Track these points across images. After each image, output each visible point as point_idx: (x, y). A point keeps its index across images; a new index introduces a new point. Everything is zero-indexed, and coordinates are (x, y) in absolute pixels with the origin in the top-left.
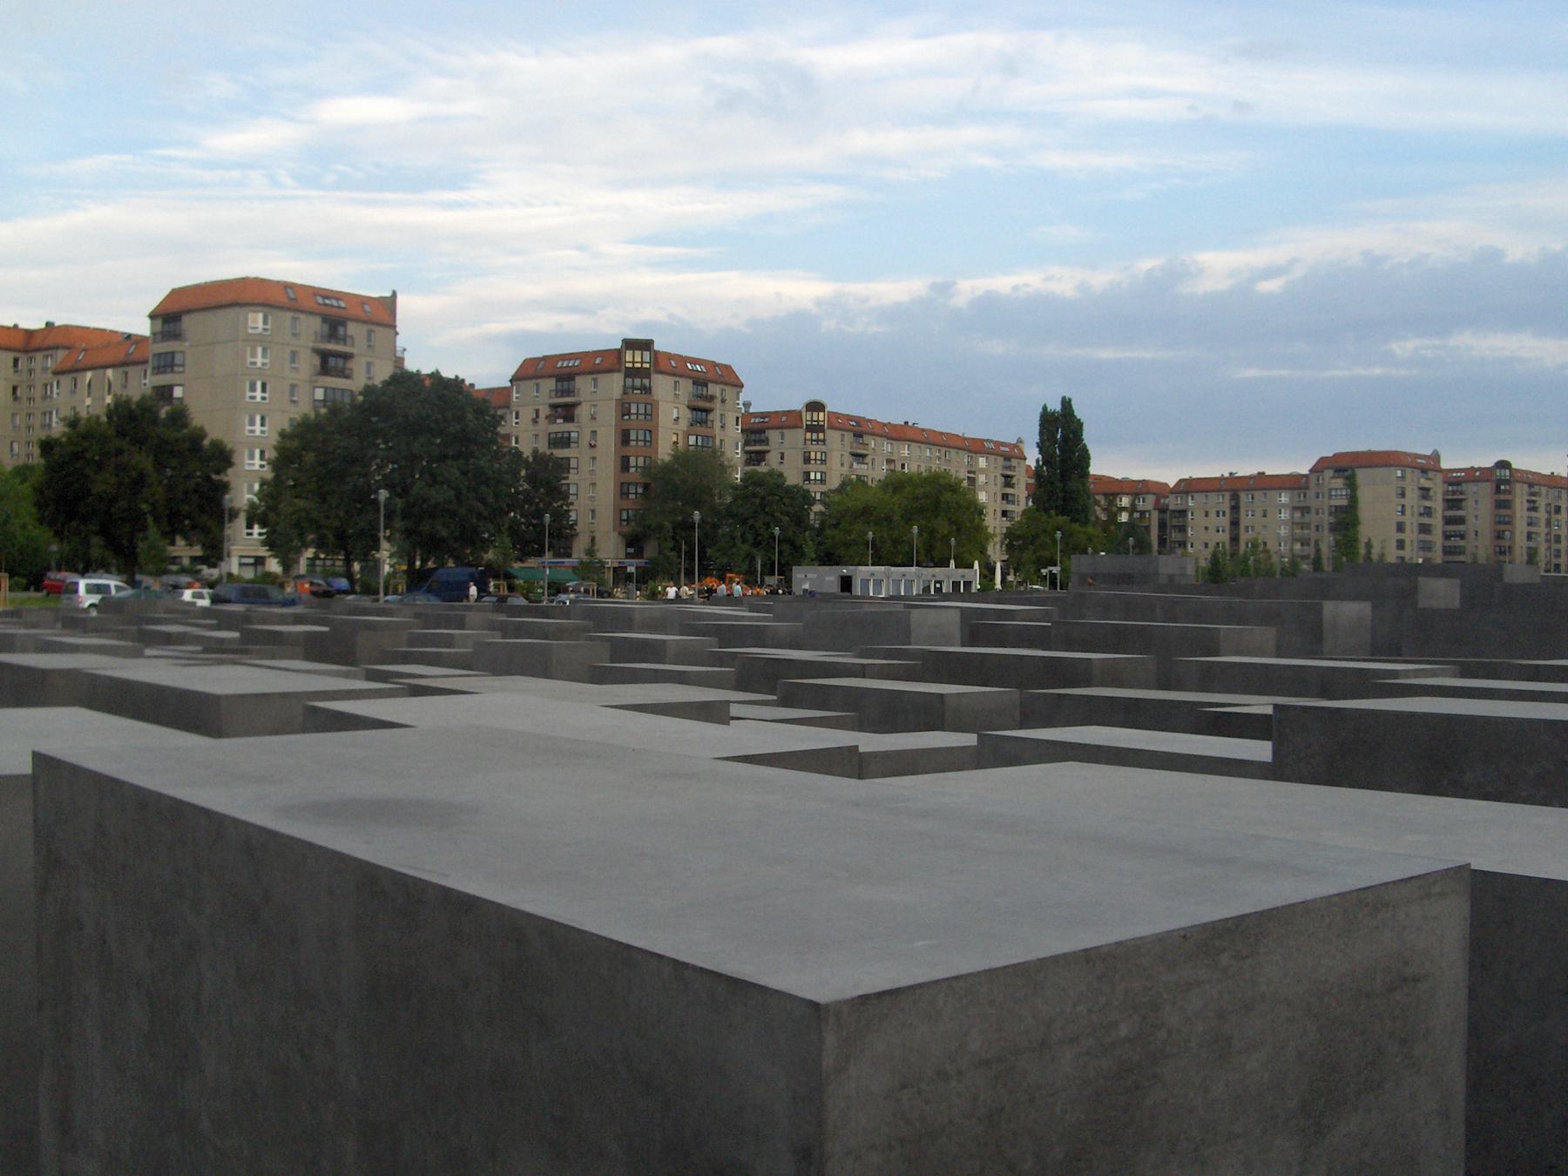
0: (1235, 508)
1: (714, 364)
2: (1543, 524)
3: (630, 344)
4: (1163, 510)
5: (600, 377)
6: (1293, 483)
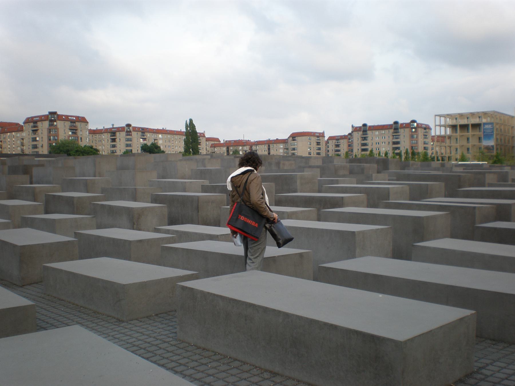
0: (269, 149)
1: (79, 117)
2: (430, 149)
5: (43, 122)
6: (284, 141)
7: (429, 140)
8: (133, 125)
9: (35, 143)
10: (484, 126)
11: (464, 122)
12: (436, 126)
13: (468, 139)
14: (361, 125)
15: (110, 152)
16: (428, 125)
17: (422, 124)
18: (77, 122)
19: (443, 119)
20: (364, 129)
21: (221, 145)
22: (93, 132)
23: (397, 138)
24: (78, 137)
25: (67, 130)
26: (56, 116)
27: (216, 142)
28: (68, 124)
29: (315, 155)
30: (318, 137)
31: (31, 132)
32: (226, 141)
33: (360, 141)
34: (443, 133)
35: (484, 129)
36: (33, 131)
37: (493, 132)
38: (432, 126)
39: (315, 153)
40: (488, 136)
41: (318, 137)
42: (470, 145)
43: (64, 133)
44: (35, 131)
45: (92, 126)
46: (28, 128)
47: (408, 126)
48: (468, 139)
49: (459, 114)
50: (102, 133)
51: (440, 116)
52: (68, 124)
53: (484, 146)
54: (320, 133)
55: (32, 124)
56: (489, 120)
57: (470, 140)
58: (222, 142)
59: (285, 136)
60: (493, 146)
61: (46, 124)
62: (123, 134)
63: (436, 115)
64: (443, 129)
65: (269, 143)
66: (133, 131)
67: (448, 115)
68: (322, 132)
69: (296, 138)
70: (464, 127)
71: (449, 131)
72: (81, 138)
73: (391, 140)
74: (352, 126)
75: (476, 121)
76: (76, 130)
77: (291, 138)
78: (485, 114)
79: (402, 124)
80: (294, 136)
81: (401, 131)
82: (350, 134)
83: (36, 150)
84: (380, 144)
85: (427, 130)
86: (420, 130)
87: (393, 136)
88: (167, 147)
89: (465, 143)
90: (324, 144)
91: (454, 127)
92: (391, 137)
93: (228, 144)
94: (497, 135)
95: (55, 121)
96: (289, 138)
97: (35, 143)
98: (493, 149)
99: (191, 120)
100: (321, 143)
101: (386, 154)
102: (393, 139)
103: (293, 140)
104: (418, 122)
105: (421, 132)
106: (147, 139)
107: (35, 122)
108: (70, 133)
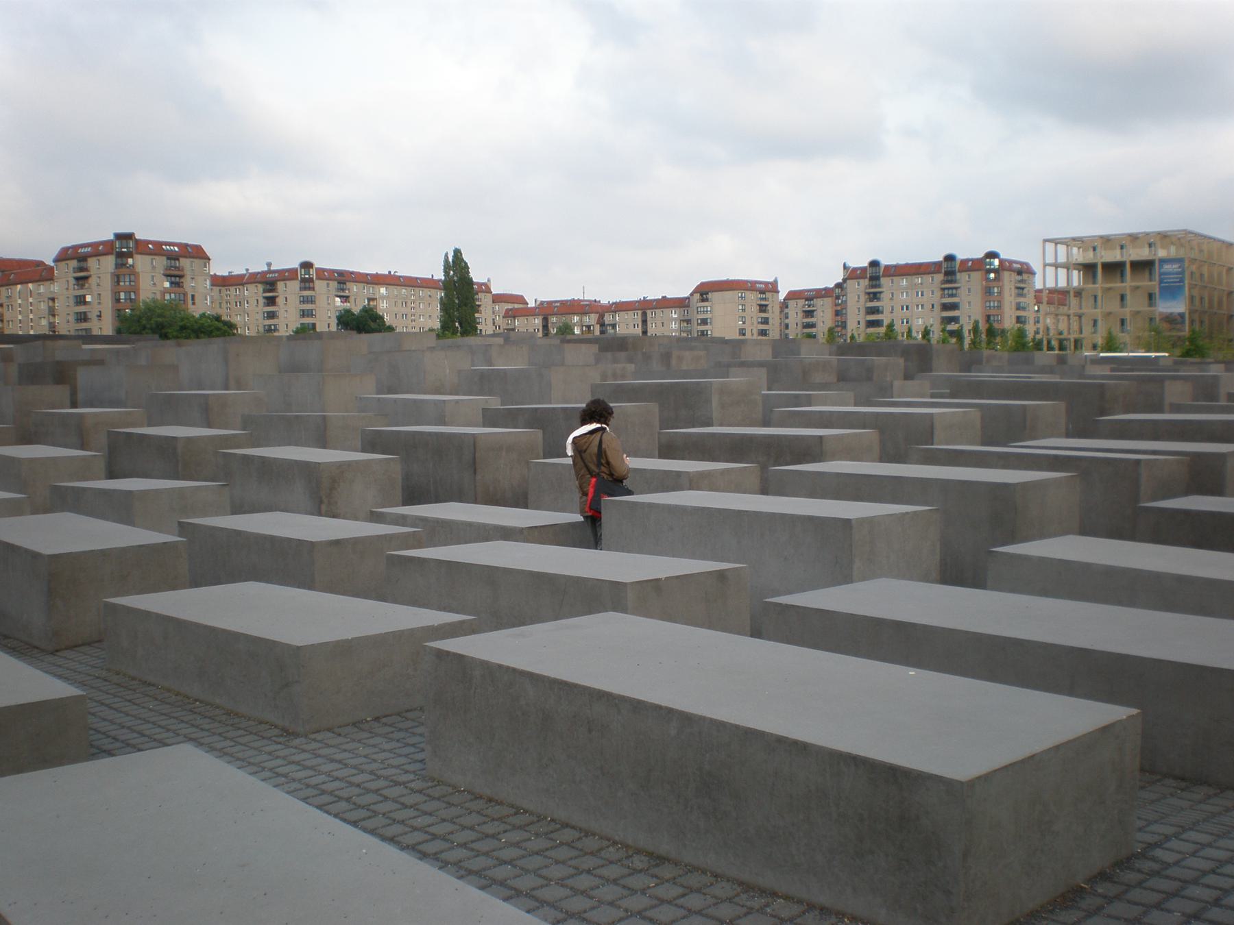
0: (644, 322)
1: (187, 245)
2: (1032, 322)
3: (119, 237)
4: (602, 325)
5: (101, 258)
6: (681, 303)
7: (1029, 299)
8: (317, 265)
9: (82, 309)
10: (1161, 267)
11: (1114, 256)
12: (1045, 265)
13: (1122, 298)
14: (866, 264)
15: (261, 330)
16: (1027, 264)
17: (1011, 262)
18: (181, 258)
19: (1062, 249)
20: (874, 274)
21: (530, 313)
22: (222, 282)
23: (952, 296)
24: (185, 294)
25: (159, 277)
26: (131, 244)
27: (516, 306)
28: (161, 262)
29: (755, 337)
30: (762, 292)
31: (72, 281)
32: (542, 303)
33: (863, 303)
34: (1062, 283)
35: (1160, 274)
36: (77, 279)
37: (1182, 280)
38: (1036, 266)
39: (755, 332)
40: (1171, 291)
41: (762, 292)
42: (1126, 312)
43: (151, 284)
44: (81, 281)
45: (219, 268)
46: (67, 272)
47: (977, 265)
48: (1122, 298)
49: (1101, 237)
50: (243, 285)
51: (1056, 242)
52: (161, 262)
53: (1161, 314)
54: (767, 284)
55: (74, 263)
56: (1173, 252)
57: (1128, 297)
58: (531, 304)
59: (683, 290)
60: (1182, 315)
61: (109, 262)
62: (294, 286)
63: (1045, 241)
64: (1062, 272)
65: (644, 307)
66: (319, 278)
67: (1074, 239)
68: (771, 280)
69: (710, 296)
70: (1113, 269)
71: (1076, 279)
72: (193, 296)
73: (937, 298)
74: (845, 267)
75: (1143, 254)
76: (181, 277)
77: (697, 296)
78: (1164, 237)
79: (964, 262)
80: (705, 291)
81: (962, 277)
82: (838, 286)
83: (84, 325)
84: (912, 310)
85: (1025, 276)
86: (1006, 275)
87: (943, 289)
88: (399, 316)
89: (1114, 306)
90: (777, 309)
91: (1088, 269)
92: (938, 293)
93: (546, 310)
94: (1192, 287)
95: (130, 255)
96: (692, 294)
97: (82, 309)
98: (1183, 322)
99: (457, 253)
100: (769, 308)
101: (926, 333)
102: (943, 296)
103: (703, 300)
104: (1002, 257)
105: (1009, 279)
106: (352, 300)
107: (83, 259)
108: (167, 285)
